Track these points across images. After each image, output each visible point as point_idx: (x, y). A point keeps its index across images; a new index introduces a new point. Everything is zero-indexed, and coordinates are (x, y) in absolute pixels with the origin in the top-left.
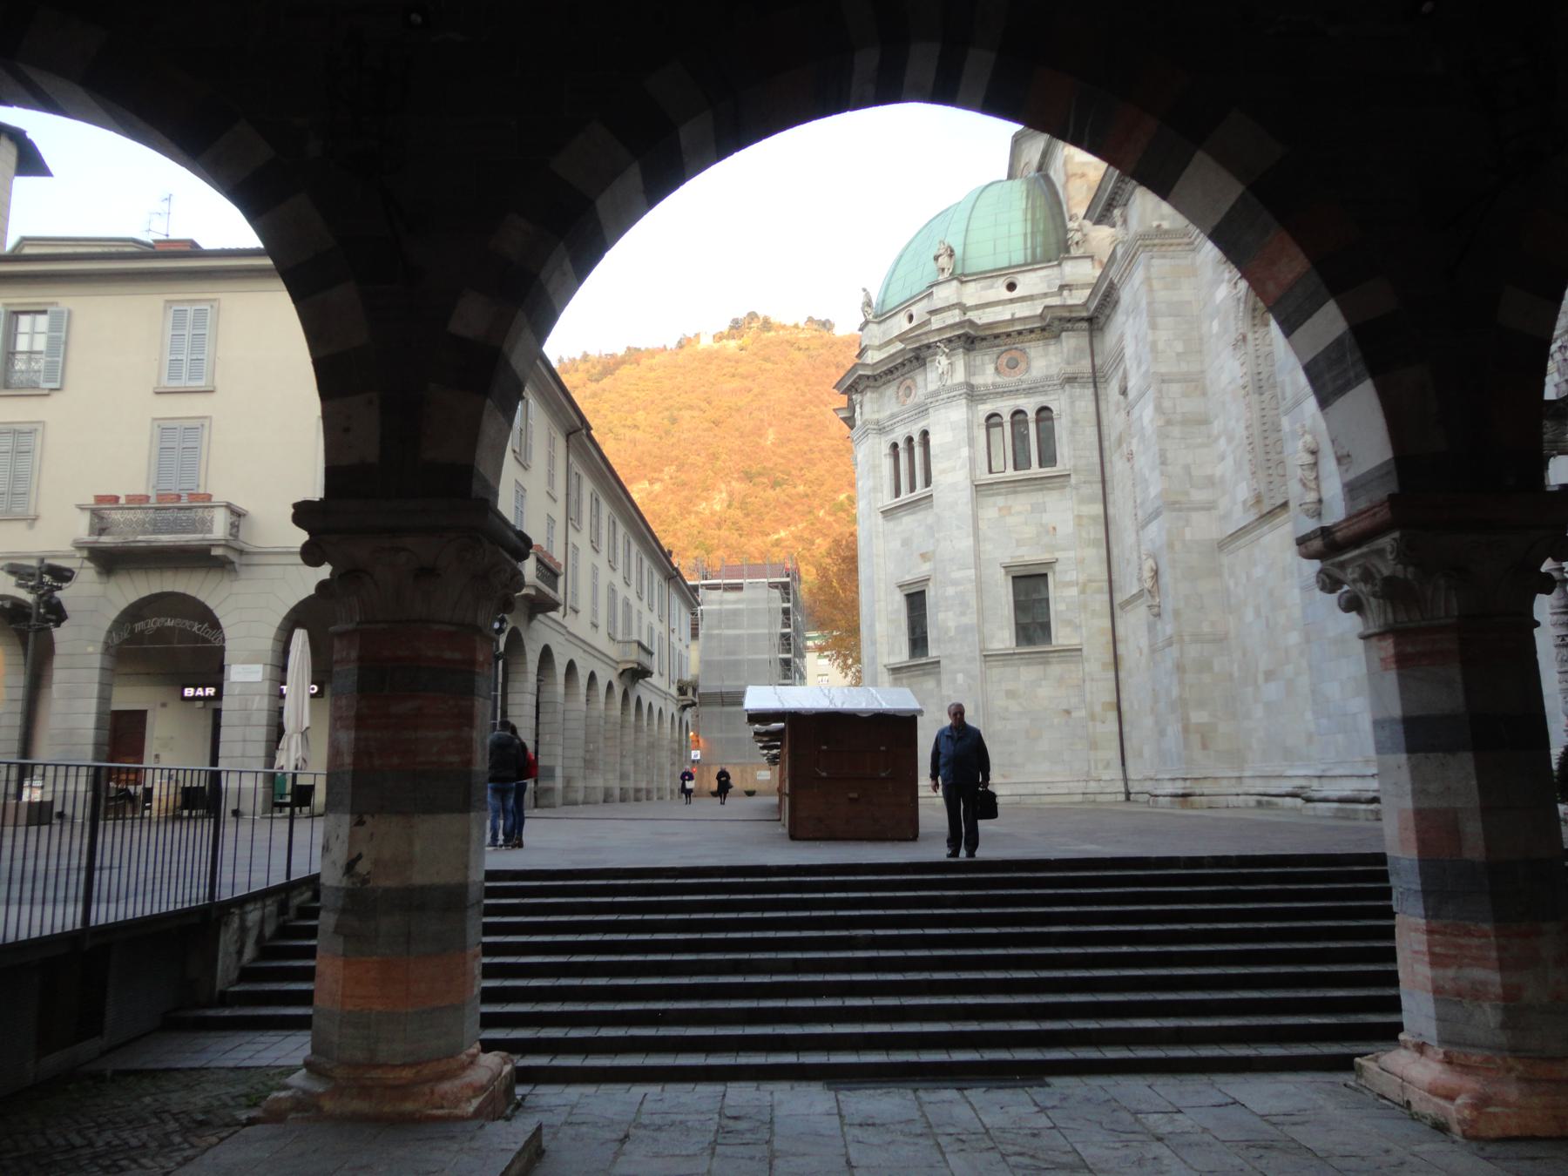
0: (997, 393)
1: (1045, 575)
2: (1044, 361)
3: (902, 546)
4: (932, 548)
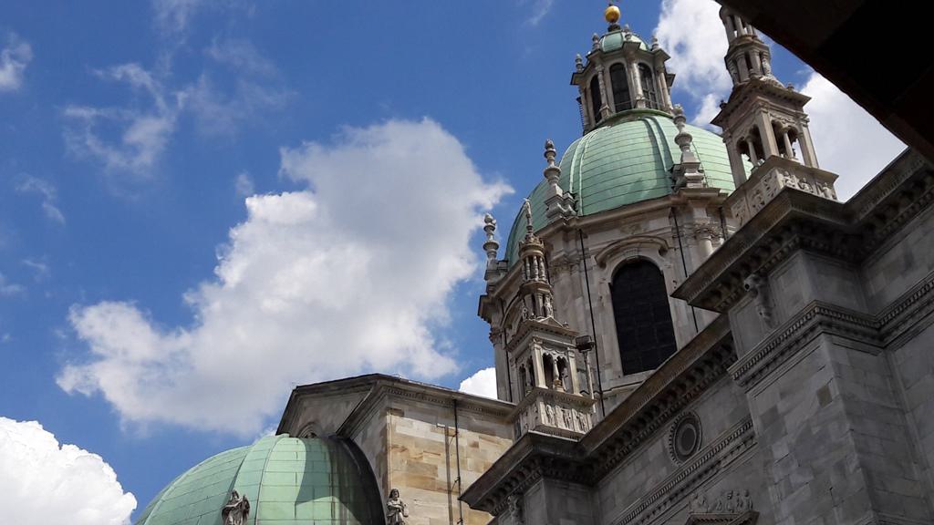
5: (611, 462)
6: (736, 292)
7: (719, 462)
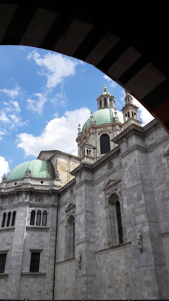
1: (40, 253)
2: (47, 201)
3: (2, 240)
4: (11, 242)
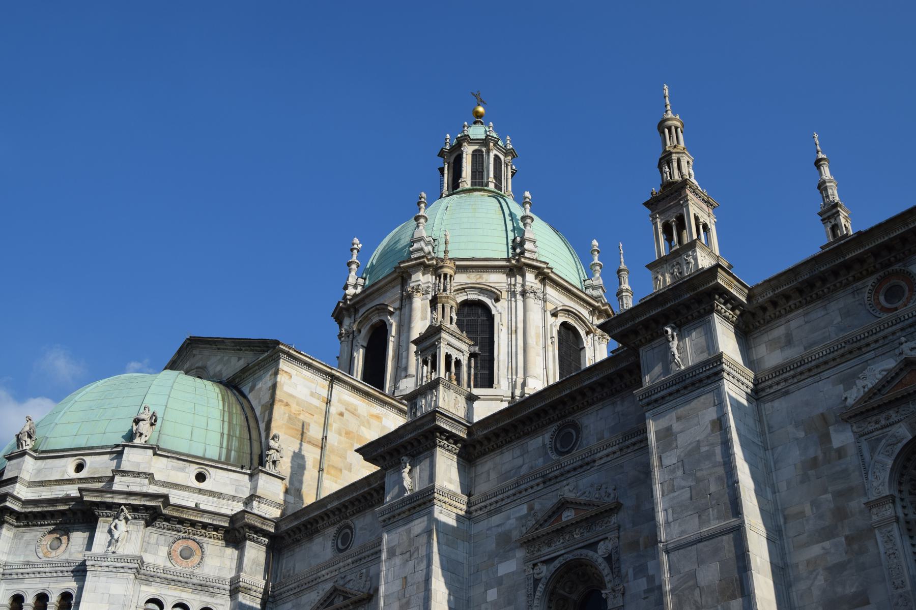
0: (166, 579)
5: (493, 446)
6: (652, 335)
7: (594, 461)
